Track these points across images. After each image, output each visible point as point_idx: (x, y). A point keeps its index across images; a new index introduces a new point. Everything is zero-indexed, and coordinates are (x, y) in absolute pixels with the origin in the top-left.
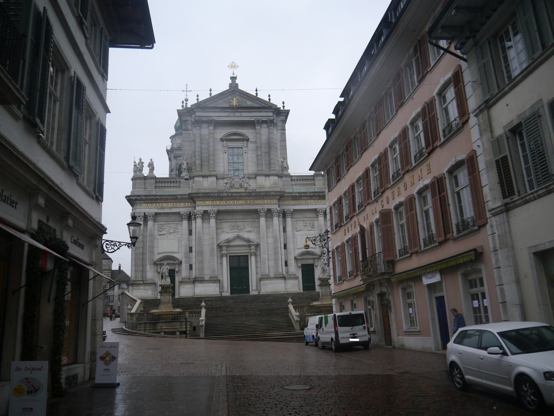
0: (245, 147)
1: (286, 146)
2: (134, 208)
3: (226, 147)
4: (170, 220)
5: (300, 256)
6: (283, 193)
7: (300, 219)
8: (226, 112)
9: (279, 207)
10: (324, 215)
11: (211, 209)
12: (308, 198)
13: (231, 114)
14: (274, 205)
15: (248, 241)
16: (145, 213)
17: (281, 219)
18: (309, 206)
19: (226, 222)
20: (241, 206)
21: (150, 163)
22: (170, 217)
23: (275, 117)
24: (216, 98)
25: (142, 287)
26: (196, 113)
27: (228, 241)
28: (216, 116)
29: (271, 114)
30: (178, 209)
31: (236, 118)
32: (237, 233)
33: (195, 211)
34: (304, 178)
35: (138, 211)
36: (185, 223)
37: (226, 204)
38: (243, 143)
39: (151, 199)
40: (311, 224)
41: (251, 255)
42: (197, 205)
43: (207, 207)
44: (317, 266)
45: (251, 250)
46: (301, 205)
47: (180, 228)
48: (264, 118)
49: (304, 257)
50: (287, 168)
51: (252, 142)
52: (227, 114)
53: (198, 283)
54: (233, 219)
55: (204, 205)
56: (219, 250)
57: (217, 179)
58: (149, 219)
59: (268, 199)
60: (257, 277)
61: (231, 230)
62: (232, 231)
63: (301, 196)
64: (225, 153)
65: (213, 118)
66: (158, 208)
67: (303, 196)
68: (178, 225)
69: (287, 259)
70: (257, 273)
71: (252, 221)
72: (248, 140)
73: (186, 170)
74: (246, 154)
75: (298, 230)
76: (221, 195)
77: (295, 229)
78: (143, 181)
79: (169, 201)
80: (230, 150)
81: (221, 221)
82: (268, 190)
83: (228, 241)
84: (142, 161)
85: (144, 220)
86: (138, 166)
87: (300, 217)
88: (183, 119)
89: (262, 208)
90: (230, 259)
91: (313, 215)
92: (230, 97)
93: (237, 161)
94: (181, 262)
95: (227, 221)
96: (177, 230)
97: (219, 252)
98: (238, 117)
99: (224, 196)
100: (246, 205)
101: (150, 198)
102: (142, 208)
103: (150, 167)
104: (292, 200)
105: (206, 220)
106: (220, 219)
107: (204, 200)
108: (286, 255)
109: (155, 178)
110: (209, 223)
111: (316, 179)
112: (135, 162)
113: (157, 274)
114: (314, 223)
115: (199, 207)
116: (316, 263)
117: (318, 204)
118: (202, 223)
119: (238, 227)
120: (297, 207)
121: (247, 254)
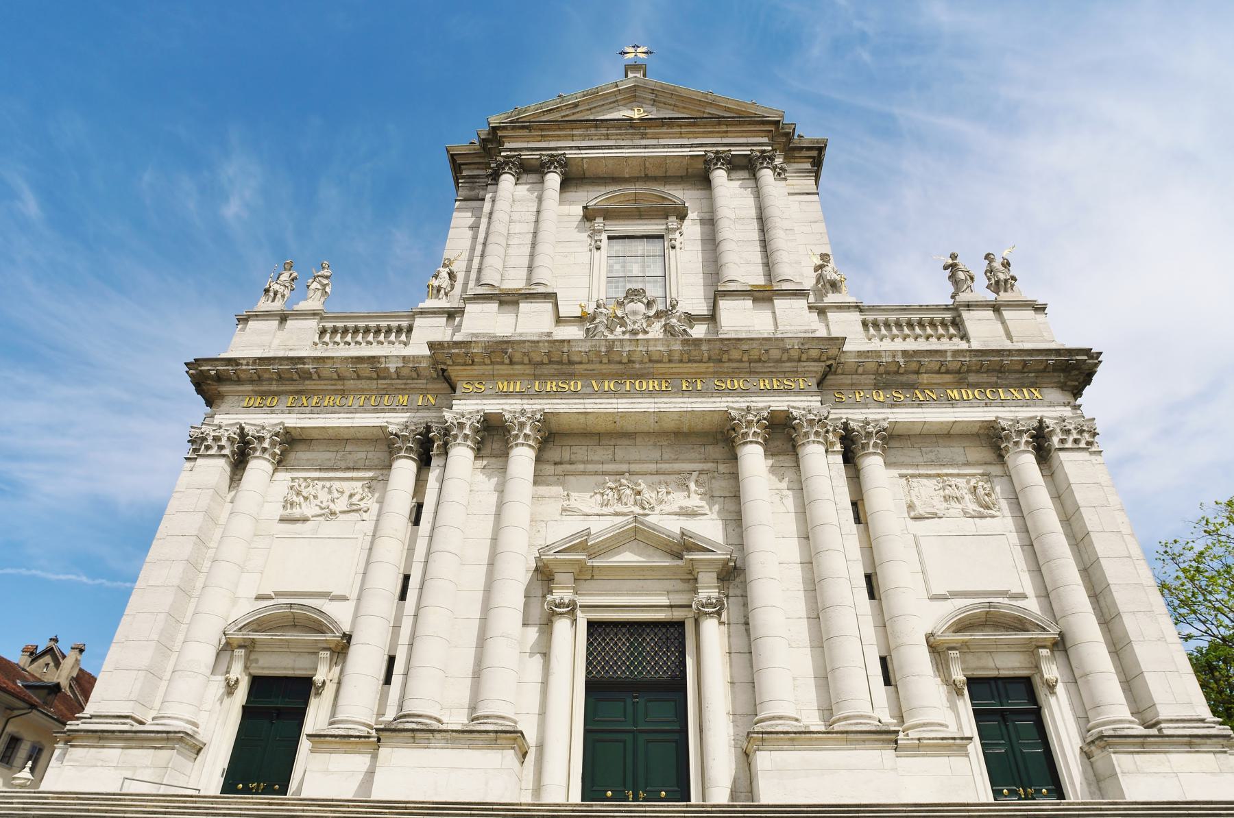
5: (956, 631)
8: (607, 137)
9: (822, 404)
10: (1034, 448)
11: (518, 408)
12: (948, 378)
15: (682, 547)
19: (584, 473)
22: (350, 452)
28: (571, 148)
29: (765, 140)
31: (644, 150)
36: (405, 469)
37: (589, 390)
38: (664, 221)
39: (280, 377)
40: (980, 491)
42: (458, 392)
44: (1051, 687)
46: (920, 405)
48: (738, 148)
49: (979, 636)
54: (614, 461)
62: (605, 510)
64: (598, 248)
65: (560, 152)
69: (889, 650)
71: (701, 472)
73: (442, 291)
74: (672, 252)
75: (920, 510)
76: (565, 350)
80: (618, 246)
81: (560, 468)
82: (766, 336)
90: (589, 634)
91: (979, 453)
94: (348, 638)
95: (590, 467)
97: (536, 602)
101: (274, 368)
104: (877, 387)
106: (558, 460)
108: (884, 624)
111: (966, 315)
119: (639, 493)
120: (905, 415)
121: (677, 615)
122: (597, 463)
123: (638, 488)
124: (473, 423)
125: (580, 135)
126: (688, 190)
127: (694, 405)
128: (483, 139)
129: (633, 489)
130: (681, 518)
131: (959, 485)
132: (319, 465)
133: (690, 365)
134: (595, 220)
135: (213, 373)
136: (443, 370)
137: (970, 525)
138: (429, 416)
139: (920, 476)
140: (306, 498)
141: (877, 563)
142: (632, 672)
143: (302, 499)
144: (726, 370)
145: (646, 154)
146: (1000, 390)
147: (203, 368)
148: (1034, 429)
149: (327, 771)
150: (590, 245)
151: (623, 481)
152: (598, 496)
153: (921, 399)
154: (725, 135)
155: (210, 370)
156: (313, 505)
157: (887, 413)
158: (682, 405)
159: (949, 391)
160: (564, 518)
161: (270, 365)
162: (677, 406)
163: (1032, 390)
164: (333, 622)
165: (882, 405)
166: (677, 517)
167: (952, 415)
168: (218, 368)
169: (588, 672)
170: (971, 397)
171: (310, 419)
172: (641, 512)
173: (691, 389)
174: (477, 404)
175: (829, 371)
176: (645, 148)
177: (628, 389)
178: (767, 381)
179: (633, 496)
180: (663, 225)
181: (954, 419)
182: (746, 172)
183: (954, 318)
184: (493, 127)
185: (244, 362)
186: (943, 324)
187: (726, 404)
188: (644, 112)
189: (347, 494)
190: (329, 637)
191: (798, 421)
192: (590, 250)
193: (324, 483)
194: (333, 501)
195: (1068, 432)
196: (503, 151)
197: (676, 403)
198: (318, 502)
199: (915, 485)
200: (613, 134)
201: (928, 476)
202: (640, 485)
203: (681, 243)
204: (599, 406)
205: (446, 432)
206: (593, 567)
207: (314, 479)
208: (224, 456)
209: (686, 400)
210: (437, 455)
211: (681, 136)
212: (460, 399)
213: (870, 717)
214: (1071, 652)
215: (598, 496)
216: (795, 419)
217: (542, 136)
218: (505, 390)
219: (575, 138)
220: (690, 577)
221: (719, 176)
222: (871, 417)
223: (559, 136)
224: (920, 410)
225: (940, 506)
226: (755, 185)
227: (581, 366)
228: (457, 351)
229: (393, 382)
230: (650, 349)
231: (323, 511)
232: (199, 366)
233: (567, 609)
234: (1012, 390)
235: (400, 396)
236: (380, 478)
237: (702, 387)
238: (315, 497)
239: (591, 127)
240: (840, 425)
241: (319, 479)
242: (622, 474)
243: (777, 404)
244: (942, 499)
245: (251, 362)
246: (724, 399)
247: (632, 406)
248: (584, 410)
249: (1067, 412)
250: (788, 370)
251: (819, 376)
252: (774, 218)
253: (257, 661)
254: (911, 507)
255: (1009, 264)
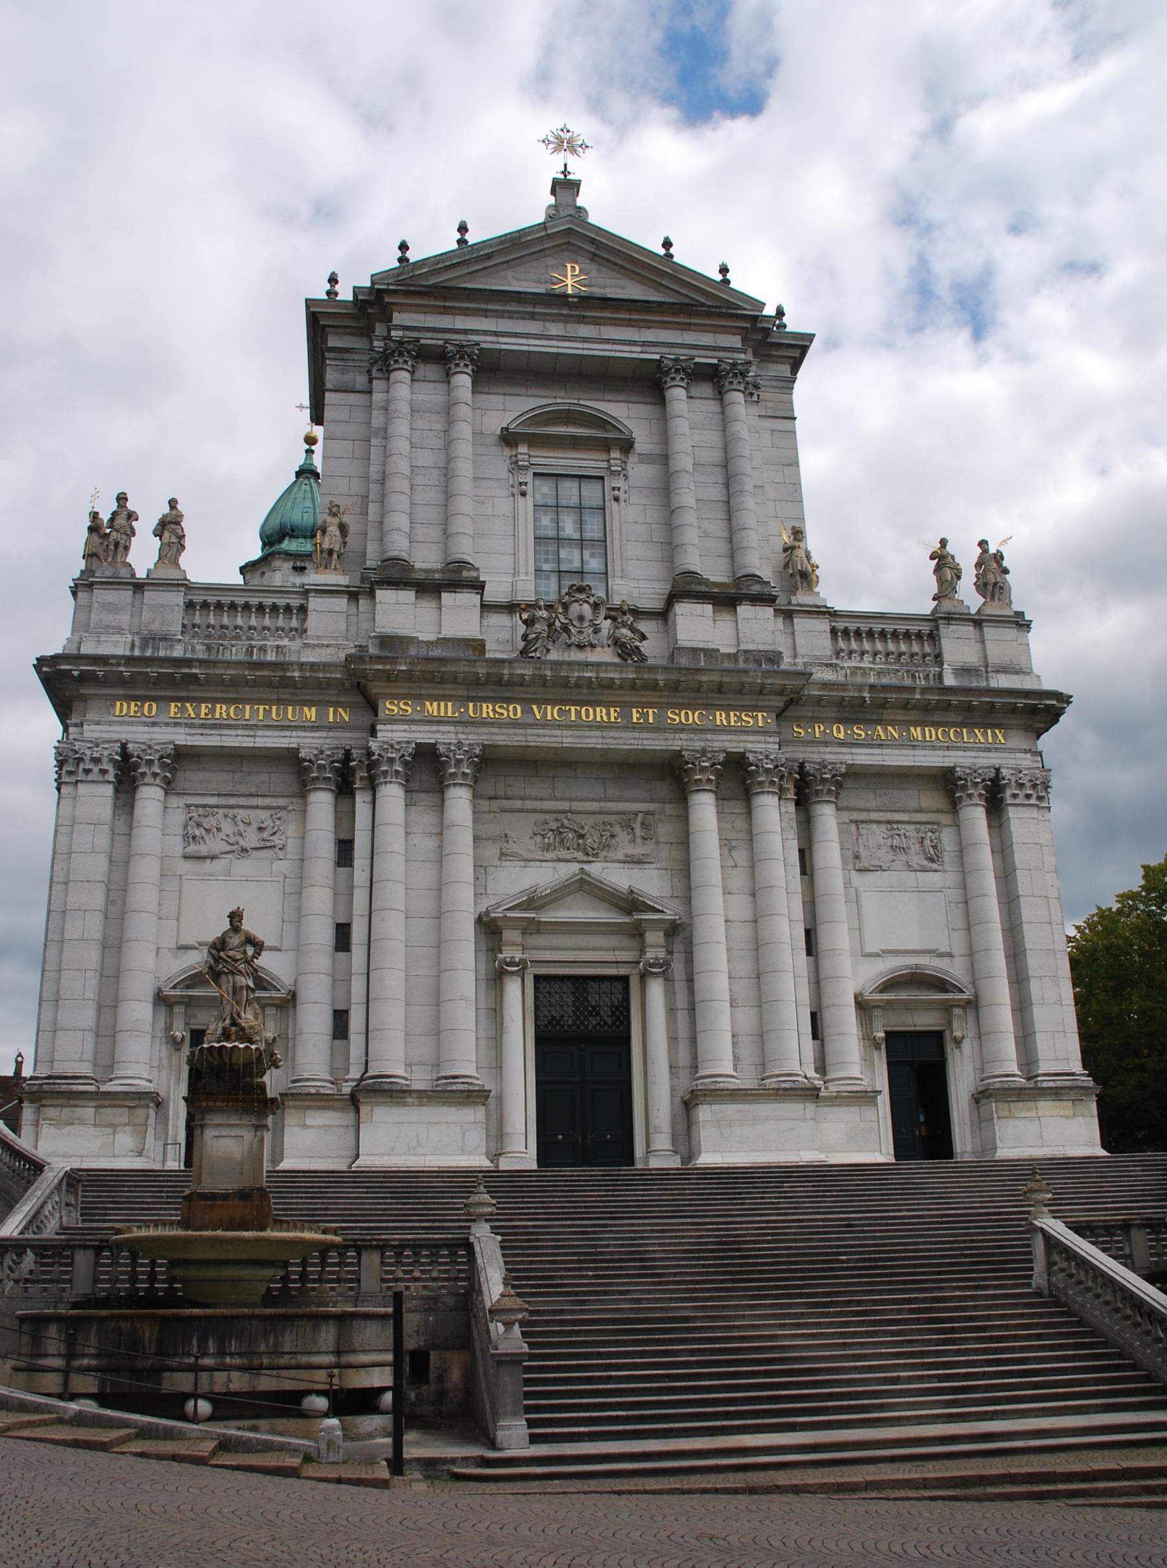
0: (613, 473)
1: (797, 485)
2: (74, 720)
3: (525, 468)
4: (243, 789)
5: (881, 992)
6: (799, 682)
7: (874, 816)
8: (533, 316)
10: (987, 801)
12: (914, 715)
13: (555, 329)
14: (761, 738)
15: (631, 903)
16: (124, 746)
17: (791, 807)
18: (917, 752)
20: (599, 733)
21: (165, 516)
22: (250, 773)
23: (750, 357)
24: (488, 257)
25: (88, 1112)
26: (395, 315)
27: (531, 900)
29: (735, 341)
30: (287, 733)
32: (574, 867)
33: (374, 745)
34: (889, 628)
35: (91, 731)
36: (322, 802)
37: (529, 720)
38: (605, 457)
40: (927, 842)
41: (644, 977)
43: (434, 728)
44: (958, 1043)
45: (642, 951)
46: (880, 746)
47: (291, 829)
48: (702, 352)
49: (903, 995)
50: (805, 577)
51: (645, 458)
52: (534, 327)
53: (377, 1104)
54: (553, 798)
55: (417, 717)
56: (484, 947)
57: (486, 607)
58: (144, 774)
59: (727, 708)
60: (673, 1089)
61: (547, 848)
62: (550, 855)
63: (884, 705)
64: (523, 494)
65: (470, 337)
66: (191, 726)
67: (893, 706)
68: (282, 814)
70: (671, 1067)
71: (647, 813)
72: (627, 446)
73: (335, 556)
75: (865, 863)
76: (506, 671)
77: (856, 862)
78: (127, 595)
79: (245, 692)
80: (545, 489)
81: (496, 804)
83: (533, 902)
84: (130, 506)
85: (116, 776)
86: (108, 531)
87: (872, 804)
88: (330, 344)
89: (698, 745)
90: (536, 988)
91: (931, 799)
92: (549, 261)
93: (576, 536)
95: (529, 804)
96: (277, 840)
98: (584, 340)
99: (521, 682)
100: (625, 728)
102: (110, 723)
103: (166, 534)
104: (840, 721)
105: (423, 796)
106: (492, 793)
107: (420, 698)
108: (817, 982)
109: (184, 585)
110: (441, 807)
111: (943, 630)
112: (95, 516)
113: (165, 1051)
114: (939, 838)
115: (395, 727)
116: (955, 1025)
117: (958, 749)
118: (406, 805)
119: (582, 836)
120: (863, 757)
121: (622, 971)
122: (536, 799)
123: (582, 832)
124: (403, 756)
125: (496, 311)
126: (634, 403)
127: (645, 742)
128: (361, 300)
129: (575, 831)
130: (626, 866)
131: (908, 834)
132: (216, 789)
133: (642, 693)
134: (517, 446)
135: (76, 673)
136: (359, 683)
137: (911, 878)
138: (347, 739)
139: (871, 822)
140: (208, 831)
141: (819, 919)
142: (578, 1027)
143: (204, 832)
144: (681, 701)
145: (585, 352)
146: (965, 730)
147: (63, 667)
148: (990, 780)
149: (305, 1125)
150: (512, 486)
151: (566, 822)
152: (538, 836)
153: (883, 737)
154: (687, 327)
155: (71, 670)
156: (218, 839)
157: (845, 754)
158: (632, 741)
159: (912, 729)
160: (504, 863)
161: (148, 667)
162: (627, 742)
163: (997, 731)
164: (275, 978)
165: (842, 744)
166: (622, 865)
167: (911, 758)
168: (81, 668)
169: (537, 1026)
170: (934, 738)
171: (202, 735)
172: (585, 858)
173: (642, 721)
174: (405, 731)
175: (790, 703)
176: (584, 342)
177: (573, 718)
178: (723, 714)
179: (575, 840)
180: (603, 461)
181: (912, 764)
182: (710, 385)
183: (932, 631)
184: (379, 290)
185: (114, 662)
186: (919, 635)
187: (680, 743)
188: (581, 271)
189: (255, 825)
190: (274, 994)
191: (754, 768)
192: (513, 495)
193: (226, 811)
194: (241, 835)
195: (1021, 786)
196: (394, 329)
197: (625, 739)
198: (222, 835)
199: (864, 832)
200: (540, 314)
201: (879, 822)
202: (582, 828)
203: (625, 492)
204: (542, 739)
205: (372, 766)
206: (540, 922)
207: (211, 807)
208: (109, 782)
209: (637, 735)
210: (361, 789)
211: (629, 323)
212: (385, 724)
213: (797, 1075)
214: (984, 1012)
215: (538, 836)
216: (751, 765)
217: (444, 307)
218: (435, 714)
219: (488, 313)
220: (637, 933)
221: (677, 395)
222: (829, 758)
223: (467, 309)
224: (879, 751)
225: (885, 856)
226: (719, 410)
227: (522, 688)
228: (380, 667)
229: (297, 691)
230: (603, 675)
231: (233, 848)
232: (56, 664)
233: (517, 968)
234: (976, 731)
235: (306, 709)
236: (290, 808)
237: (654, 719)
238: (219, 829)
239: (513, 301)
240: (797, 769)
241: (217, 807)
242: (565, 812)
243: (734, 745)
244: (889, 849)
245: (123, 662)
246: (677, 736)
247: (578, 740)
248: (525, 744)
249: (1026, 761)
250: (746, 703)
251: (779, 711)
252: (743, 477)
253: (195, 1017)
254: (857, 857)
255: (1002, 558)
